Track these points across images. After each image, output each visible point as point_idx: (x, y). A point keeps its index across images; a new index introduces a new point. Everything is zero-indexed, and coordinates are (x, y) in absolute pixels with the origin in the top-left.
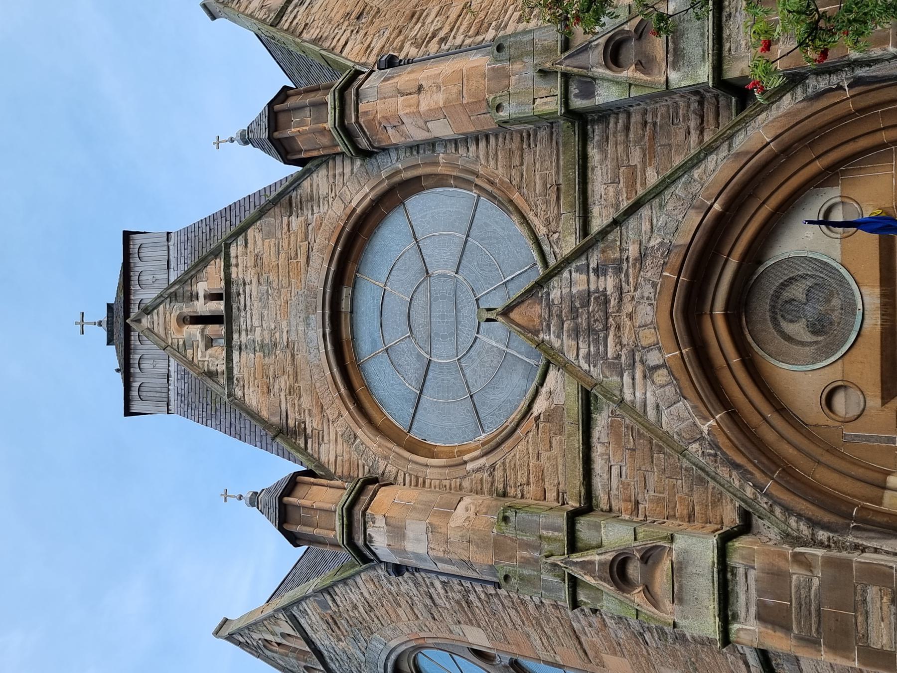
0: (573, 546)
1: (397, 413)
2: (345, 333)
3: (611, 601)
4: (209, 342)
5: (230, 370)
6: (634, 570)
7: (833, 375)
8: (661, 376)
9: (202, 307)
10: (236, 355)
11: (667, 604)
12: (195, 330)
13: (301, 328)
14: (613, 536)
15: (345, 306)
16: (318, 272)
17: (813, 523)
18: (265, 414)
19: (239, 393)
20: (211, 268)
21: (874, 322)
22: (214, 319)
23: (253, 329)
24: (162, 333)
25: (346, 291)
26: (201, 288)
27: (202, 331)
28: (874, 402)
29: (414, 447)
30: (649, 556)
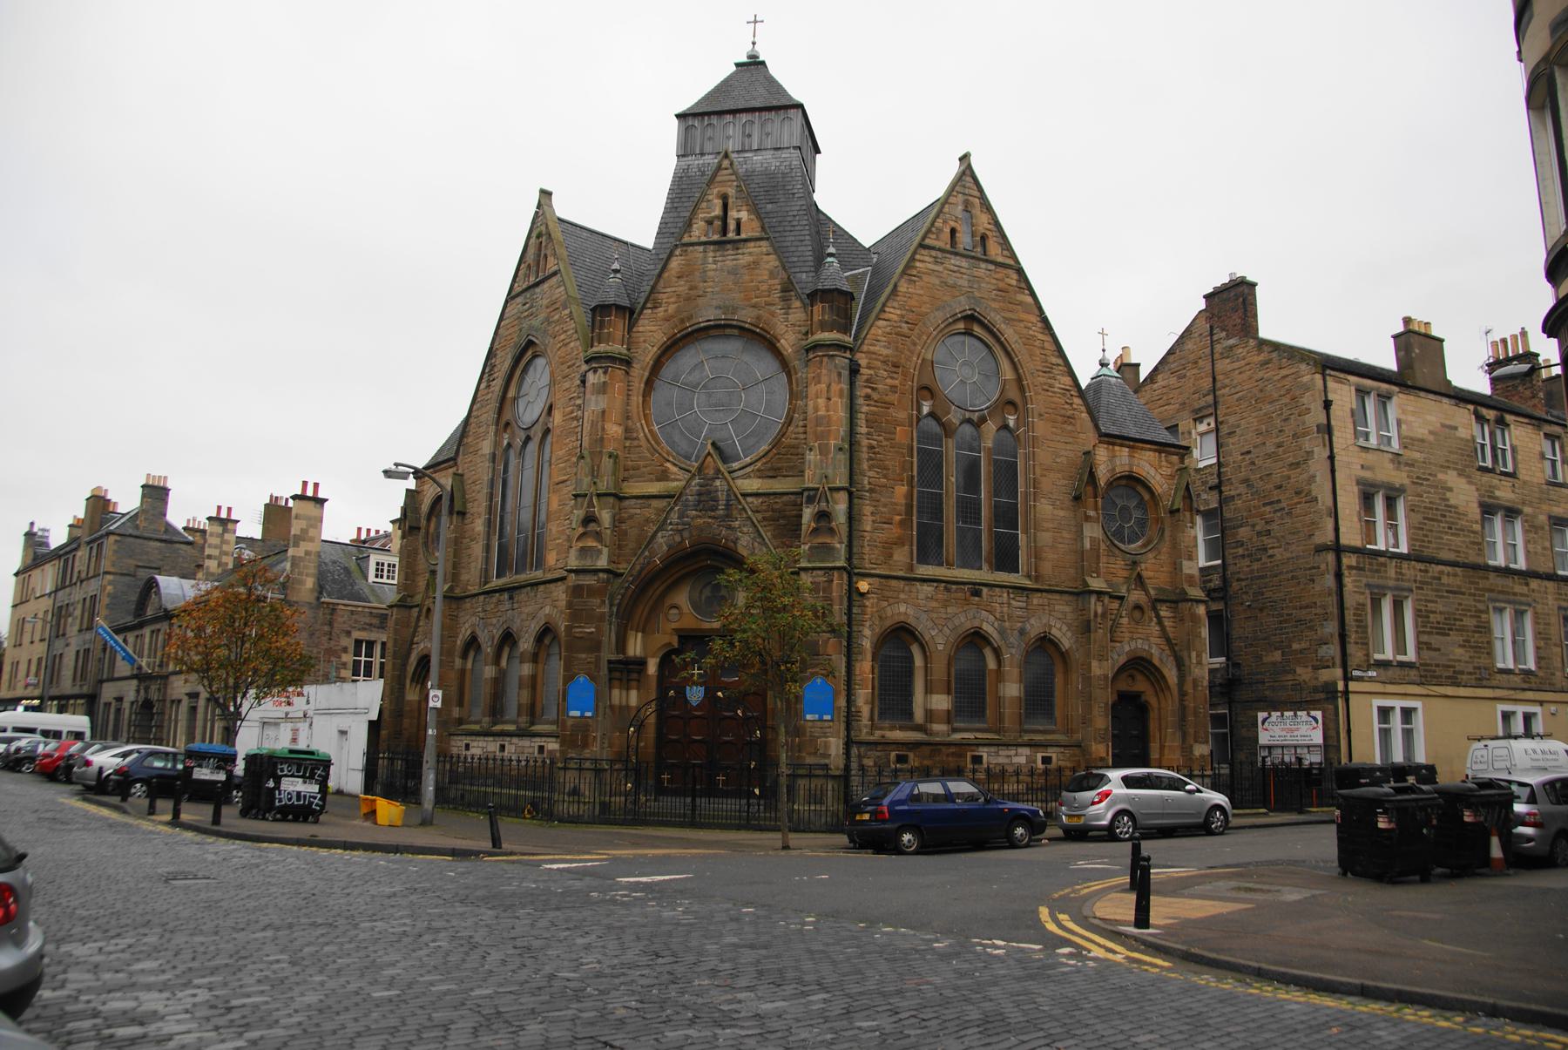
0: (599, 495)
1: (668, 371)
2: (713, 332)
3: (580, 513)
4: (710, 222)
5: (692, 244)
6: (592, 527)
7: (685, 610)
8: (678, 538)
9: (733, 214)
10: (701, 248)
11: (580, 544)
12: (718, 211)
13: (715, 303)
14: (605, 517)
15: (728, 331)
16: (746, 316)
17: (619, 605)
18: (666, 275)
19: (677, 252)
20: (756, 224)
21: (707, 626)
22: (724, 231)
23: (715, 262)
24: (718, 179)
25: (736, 332)
26: (744, 215)
27: (717, 217)
28: (674, 626)
29: (649, 384)
30: (598, 536)
